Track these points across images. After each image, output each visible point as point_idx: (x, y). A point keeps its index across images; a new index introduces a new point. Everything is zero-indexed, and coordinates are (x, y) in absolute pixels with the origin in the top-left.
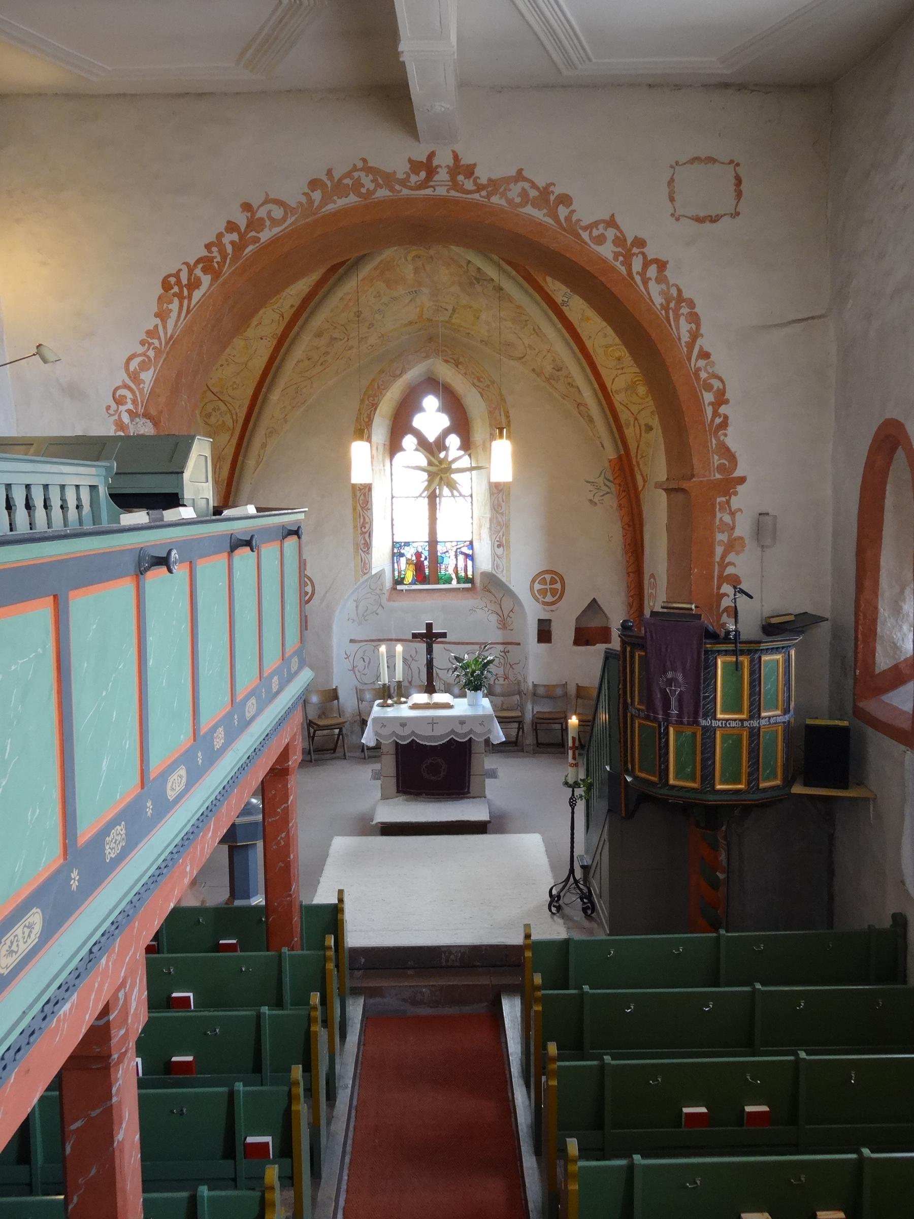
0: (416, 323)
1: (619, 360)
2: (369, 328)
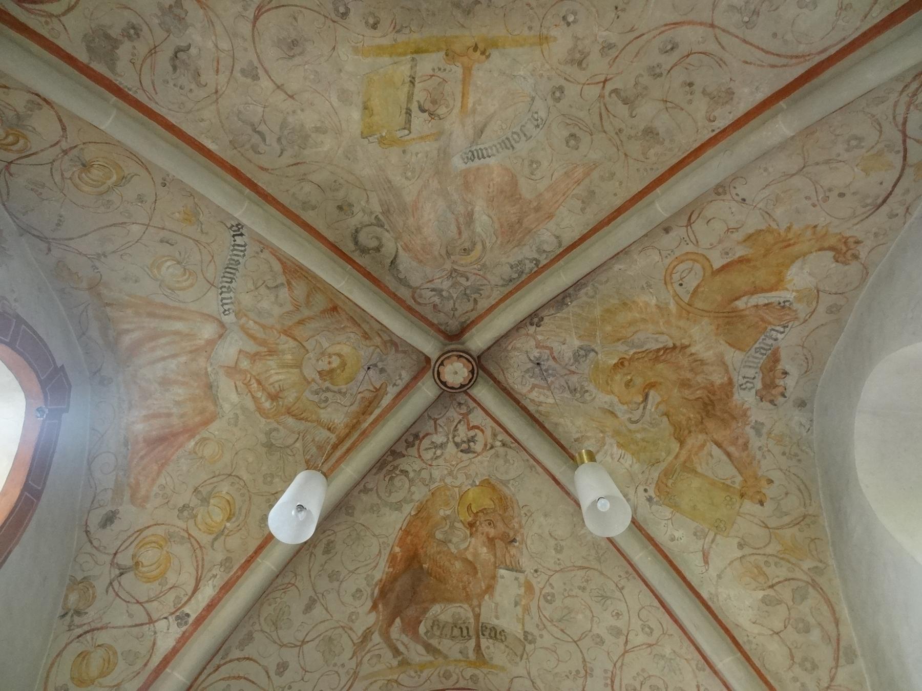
0: (476, 48)
1: (84, 165)
2: (561, 89)
